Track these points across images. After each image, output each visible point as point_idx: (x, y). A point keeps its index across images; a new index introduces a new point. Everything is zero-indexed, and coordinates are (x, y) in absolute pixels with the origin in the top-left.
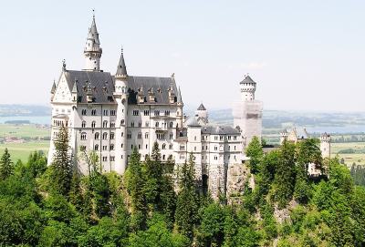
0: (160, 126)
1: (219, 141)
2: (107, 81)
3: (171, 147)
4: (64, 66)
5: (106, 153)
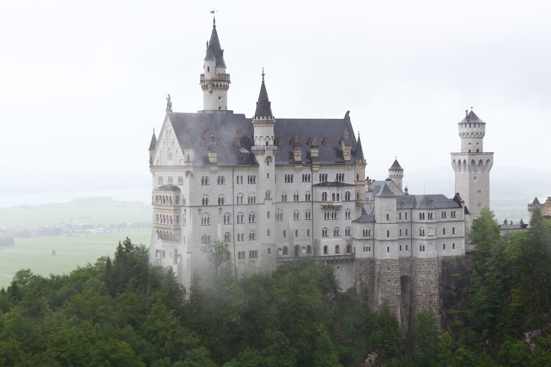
0: (329, 199)
1: (426, 220)
3: (348, 232)
4: (169, 105)
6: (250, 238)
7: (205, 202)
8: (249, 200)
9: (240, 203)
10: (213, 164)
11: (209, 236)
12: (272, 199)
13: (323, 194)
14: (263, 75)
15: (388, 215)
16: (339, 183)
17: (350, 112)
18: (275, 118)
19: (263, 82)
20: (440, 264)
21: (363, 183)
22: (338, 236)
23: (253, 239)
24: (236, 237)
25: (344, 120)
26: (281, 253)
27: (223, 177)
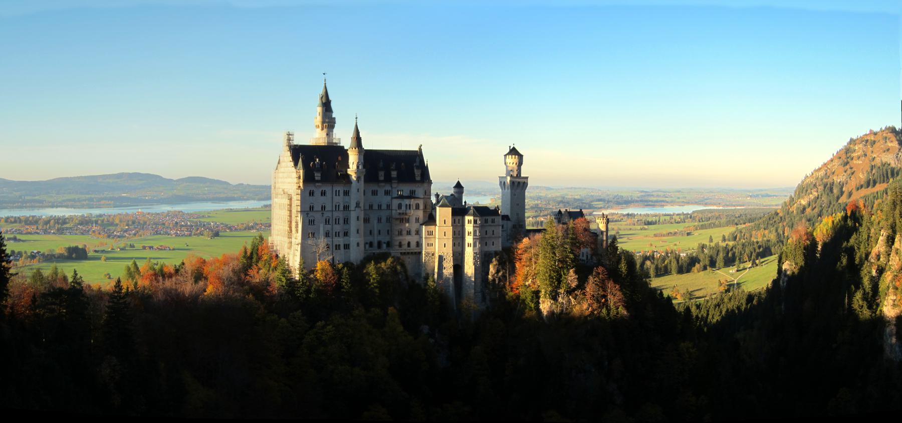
0: (403, 208)
2: (342, 153)
3: (418, 232)
4: (289, 140)
5: (340, 241)
6: (345, 236)
7: (311, 208)
8: (344, 207)
9: (337, 209)
10: (318, 181)
11: (314, 233)
12: (360, 207)
13: (399, 204)
14: (356, 118)
15: (445, 220)
16: (412, 196)
17: (421, 145)
18: (365, 149)
19: (356, 123)
20: (483, 256)
21: (428, 197)
22: (410, 234)
23: (347, 236)
24: (334, 234)
25: (417, 151)
26: (367, 246)
27: (325, 191)
